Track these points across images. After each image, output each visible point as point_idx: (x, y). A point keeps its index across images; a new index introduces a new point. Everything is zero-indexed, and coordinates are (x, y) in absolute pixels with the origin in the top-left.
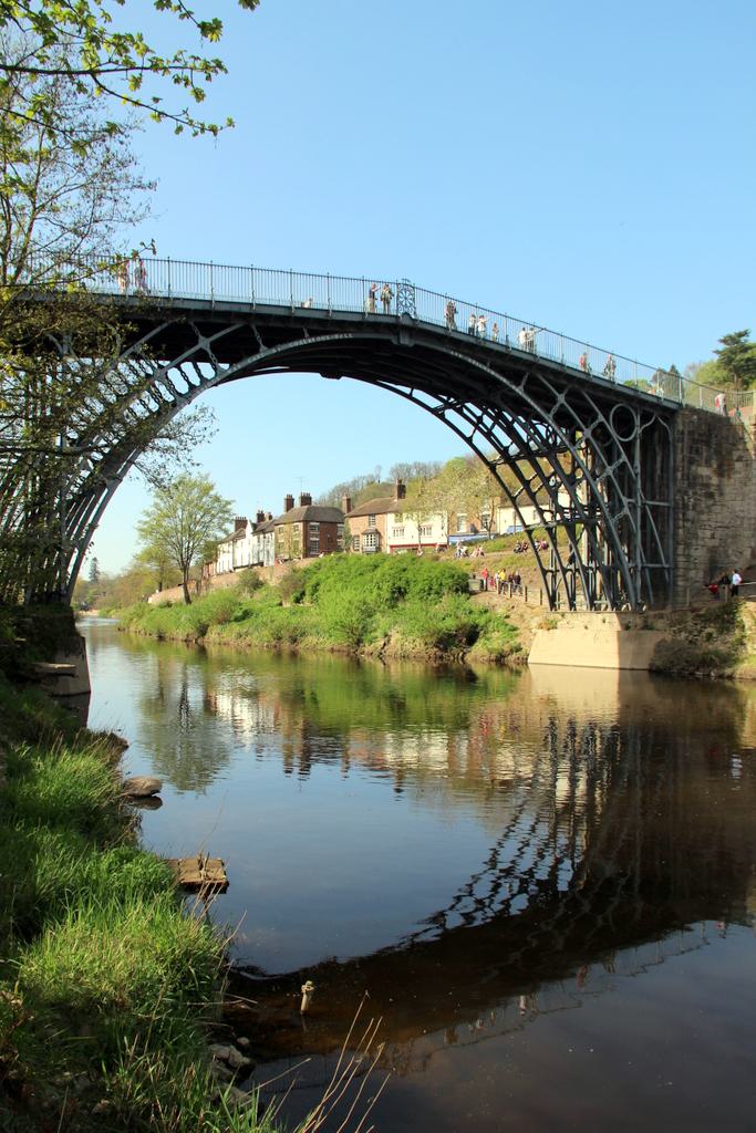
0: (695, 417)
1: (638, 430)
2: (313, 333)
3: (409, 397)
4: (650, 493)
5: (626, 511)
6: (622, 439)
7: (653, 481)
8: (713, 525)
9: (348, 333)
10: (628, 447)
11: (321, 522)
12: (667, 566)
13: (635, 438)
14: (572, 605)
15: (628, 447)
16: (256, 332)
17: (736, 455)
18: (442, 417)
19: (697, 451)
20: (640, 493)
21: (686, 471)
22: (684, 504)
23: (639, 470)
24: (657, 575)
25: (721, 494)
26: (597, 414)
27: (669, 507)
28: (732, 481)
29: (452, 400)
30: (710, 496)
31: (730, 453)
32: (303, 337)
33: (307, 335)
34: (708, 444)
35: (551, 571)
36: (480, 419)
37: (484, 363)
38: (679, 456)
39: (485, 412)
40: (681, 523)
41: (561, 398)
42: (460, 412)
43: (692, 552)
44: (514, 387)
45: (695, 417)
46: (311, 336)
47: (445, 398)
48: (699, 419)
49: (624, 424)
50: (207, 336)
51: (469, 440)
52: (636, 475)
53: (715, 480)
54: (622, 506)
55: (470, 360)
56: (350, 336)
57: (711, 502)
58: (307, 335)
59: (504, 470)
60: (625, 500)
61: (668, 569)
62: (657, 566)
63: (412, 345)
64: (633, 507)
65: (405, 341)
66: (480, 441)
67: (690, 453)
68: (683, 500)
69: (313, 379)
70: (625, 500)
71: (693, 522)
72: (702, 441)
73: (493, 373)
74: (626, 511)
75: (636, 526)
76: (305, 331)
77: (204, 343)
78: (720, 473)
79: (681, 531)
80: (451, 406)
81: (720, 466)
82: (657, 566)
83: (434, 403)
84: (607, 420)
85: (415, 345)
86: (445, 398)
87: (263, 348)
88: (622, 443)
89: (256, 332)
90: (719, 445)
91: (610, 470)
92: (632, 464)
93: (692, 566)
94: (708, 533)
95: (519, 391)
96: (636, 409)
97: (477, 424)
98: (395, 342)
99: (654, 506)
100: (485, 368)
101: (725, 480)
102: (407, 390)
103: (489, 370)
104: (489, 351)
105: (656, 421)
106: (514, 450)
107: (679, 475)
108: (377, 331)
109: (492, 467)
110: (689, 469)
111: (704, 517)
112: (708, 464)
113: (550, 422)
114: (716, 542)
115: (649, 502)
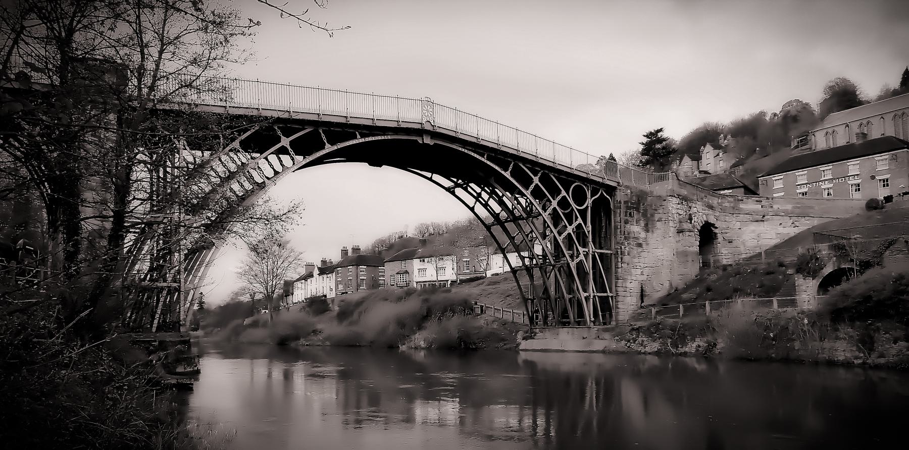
1: (589, 202)
2: (363, 136)
3: (430, 179)
4: (598, 244)
5: (582, 257)
6: (578, 208)
7: (600, 237)
8: (642, 265)
9: (388, 135)
10: (583, 213)
11: (367, 266)
12: (610, 294)
13: (587, 207)
14: (545, 323)
15: (583, 213)
16: (322, 134)
17: (657, 217)
18: (453, 193)
19: (630, 214)
20: (591, 245)
21: (623, 229)
22: (621, 251)
23: (590, 229)
24: (604, 301)
25: (647, 244)
26: (561, 191)
27: (611, 254)
28: (655, 235)
29: (460, 181)
30: (640, 245)
31: (652, 215)
32: (355, 137)
33: (358, 136)
34: (638, 210)
35: (530, 299)
36: (479, 195)
37: (483, 157)
38: (618, 218)
39: (483, 189)
40: (620, 264)
41: (536, 180)
42: (466, 190)
43: (629, 285)
44: (503, 172)
45: (629, 191)
46: (362, 137)
47: (455, 180)
48: (632, 193)
49: (580, 198)
50: (287, 136)
51: (472, 209)
52: (588, 232)
53: (643, 235)
54: (579, 254)
55: (473, 154)
56: (389, 137)
57: (640, 249)
58: (358, 136)
59: (497, 230)
60: (581, 249)
61: (612, 297)
62: (605, 294)
64: (586, 256)
65: (428, 140)
66: (480, 209)
67: (626, 216)
68: (621, 248)
69: (364, 166)
70: (581, 249)
71: (628, 264)
72: (634, 208)
73: (489, 163)
74: (582, 257)
75: (589, 266)
76: (358, 134)
77: (285, 142)
78: (647, 229)
79: (620, 270)
80: (457, 185)
81: (646, 225)
82: (605, 294)
83: (447, 183)
84: (568, 194)
86: (455, 180)
87: (327, 145)
88: (576, 208)
89: (322, 134)
90: (646, 211)
91: (570, 229)
92: (585, 224)
93: (628, 294)
94: (639, 271)
95: (507, 175)
96: (586, 185)
97: (478, 197)
98: (421, 142)
99: (601, 253)
100: (483, 160)
101: (650, 234)
102: (429, 175)
103: (486, 161)
105: (602, 192)
106: (504, 215)
107: (619, 230)
108: (408, 134)
109: (488, 228)
111: (636, 260)
113: (529, 196)
114: (644, 278)
115: (596, 250)
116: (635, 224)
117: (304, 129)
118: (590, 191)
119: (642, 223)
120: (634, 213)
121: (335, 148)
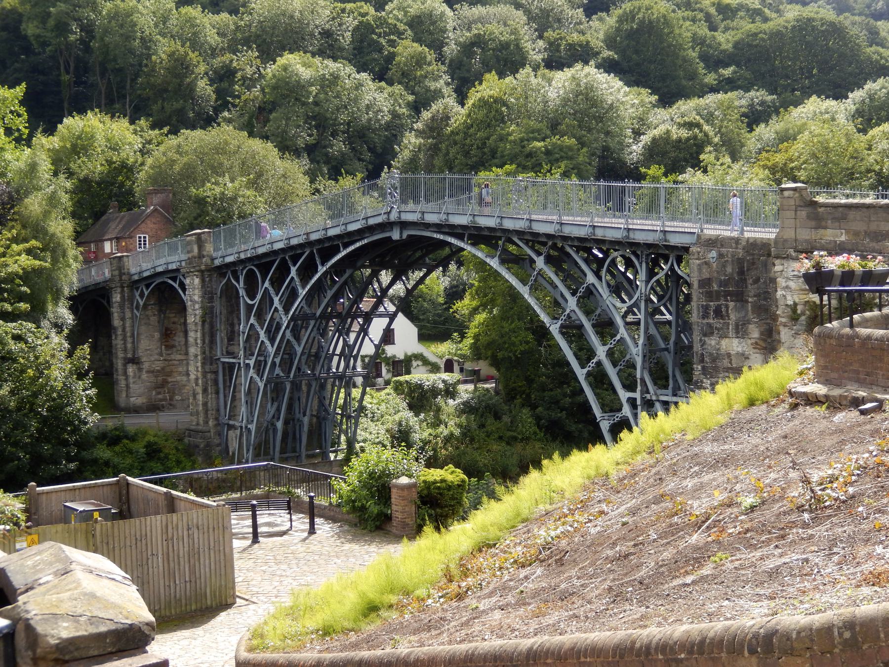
0: (714, 253)
2: (346, 246)
9: (363, 239)
19: (718, 313)
32: (339, 251)
44: (488, 260)
45: (714, 253)
56: (366, 241)
63: (404, 237)
65: (396, 235)
67: (705, 315)
72: (727, 294)
74: (626, 411)
85: (409, 236)
87: (320, 267)
104: (453, 226)
110: (703, 344)
112: (741, 331)
116: (731, 333)
117: (304, 253)
118: (644, 265)
119: (755, 333)
120: (727, 307)
121: (325, 269)
